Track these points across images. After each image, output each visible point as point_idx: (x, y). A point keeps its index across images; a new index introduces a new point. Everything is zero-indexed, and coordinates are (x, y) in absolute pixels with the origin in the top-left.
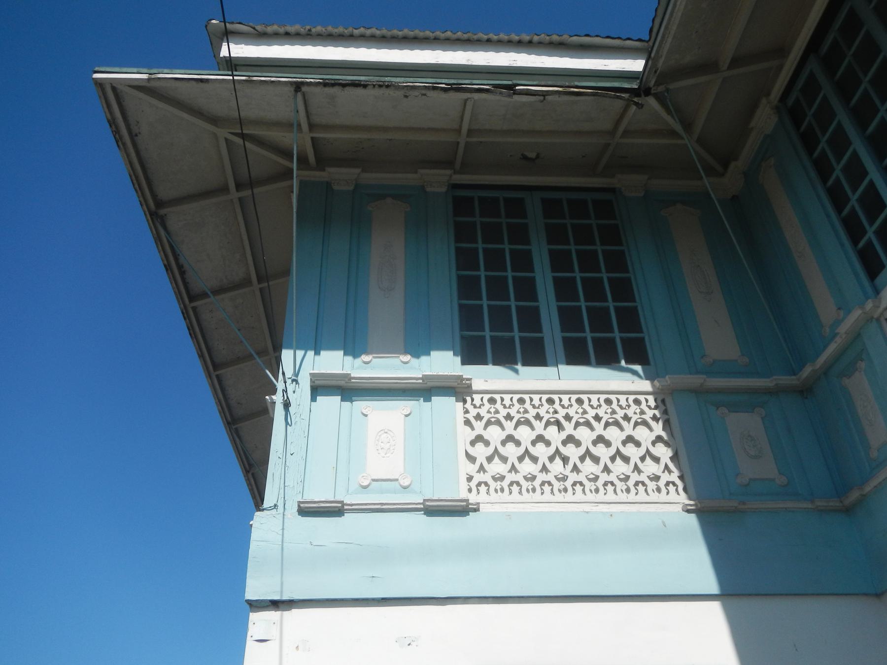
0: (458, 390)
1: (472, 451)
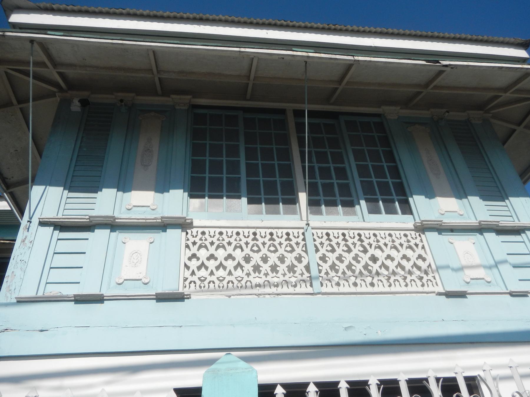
0: (184, 225)
1: (188, 263)
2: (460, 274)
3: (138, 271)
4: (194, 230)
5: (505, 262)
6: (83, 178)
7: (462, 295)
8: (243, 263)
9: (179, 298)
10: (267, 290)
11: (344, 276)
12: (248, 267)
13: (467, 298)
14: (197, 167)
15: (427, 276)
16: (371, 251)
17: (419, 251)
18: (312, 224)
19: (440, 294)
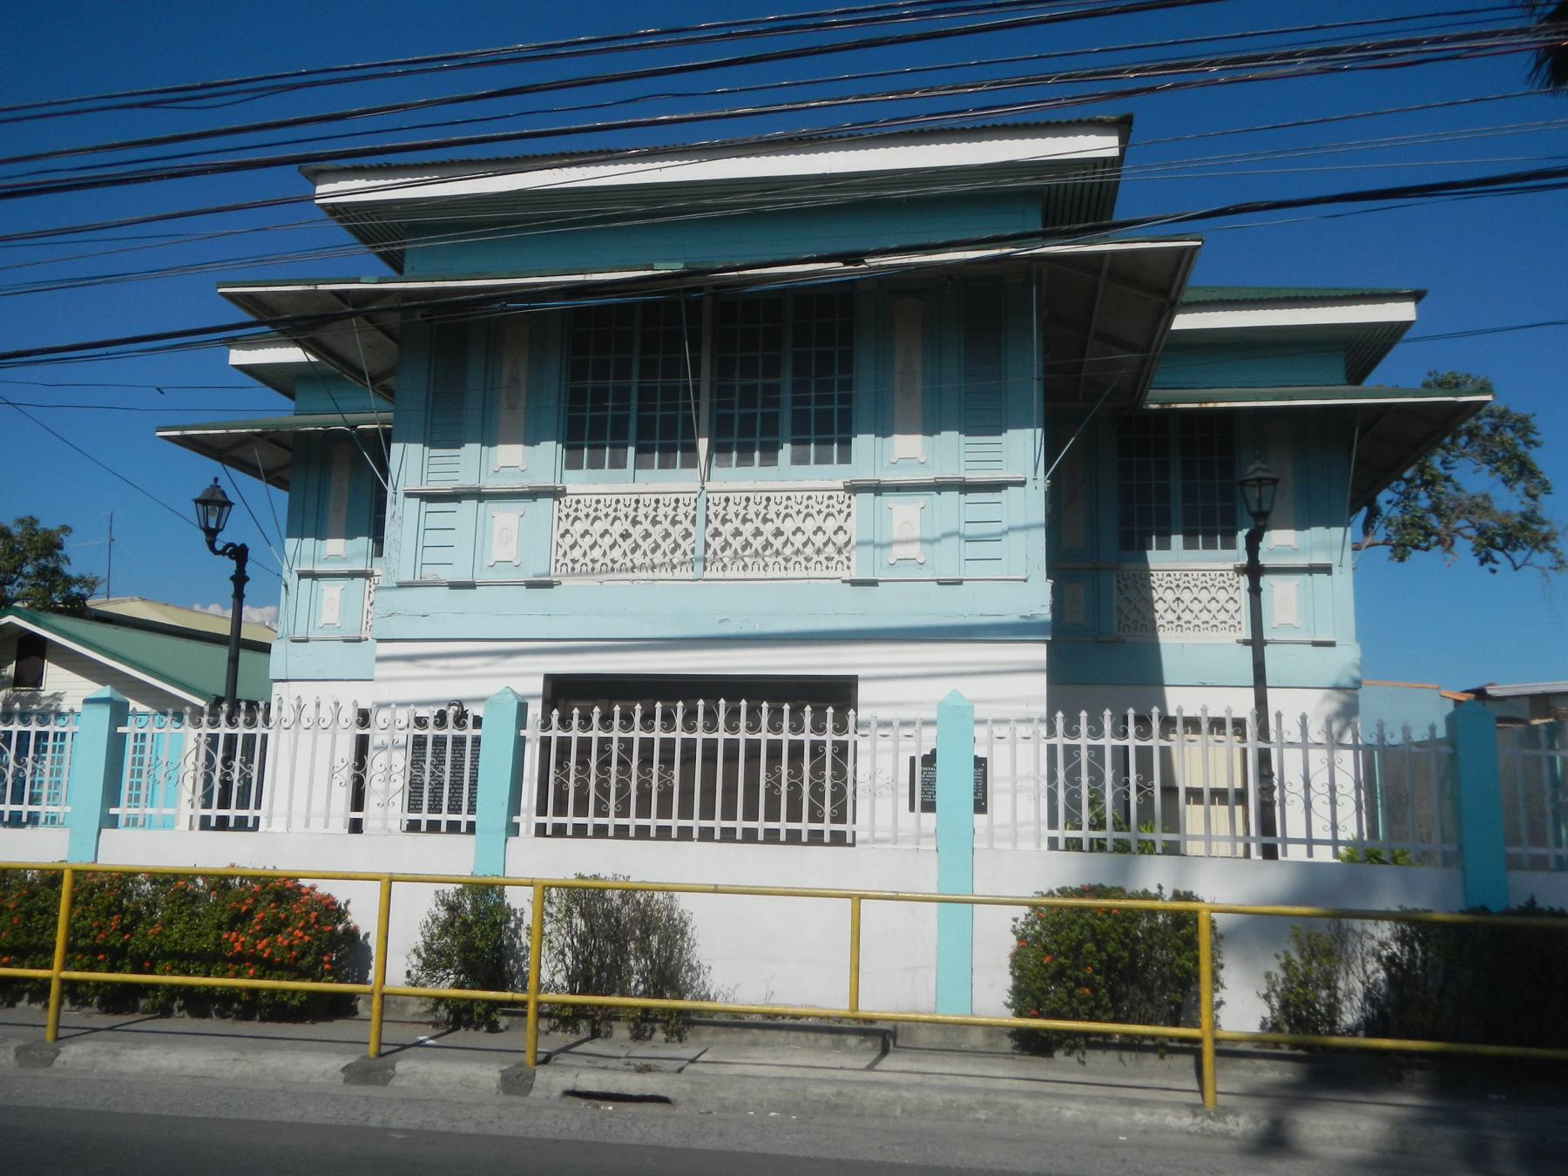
0: (556, 494)
2: (886, 551)
4: (568, 498)
6: (444, 432)
9: (549, 585)
14: (576, 398)
18: (708, 486)
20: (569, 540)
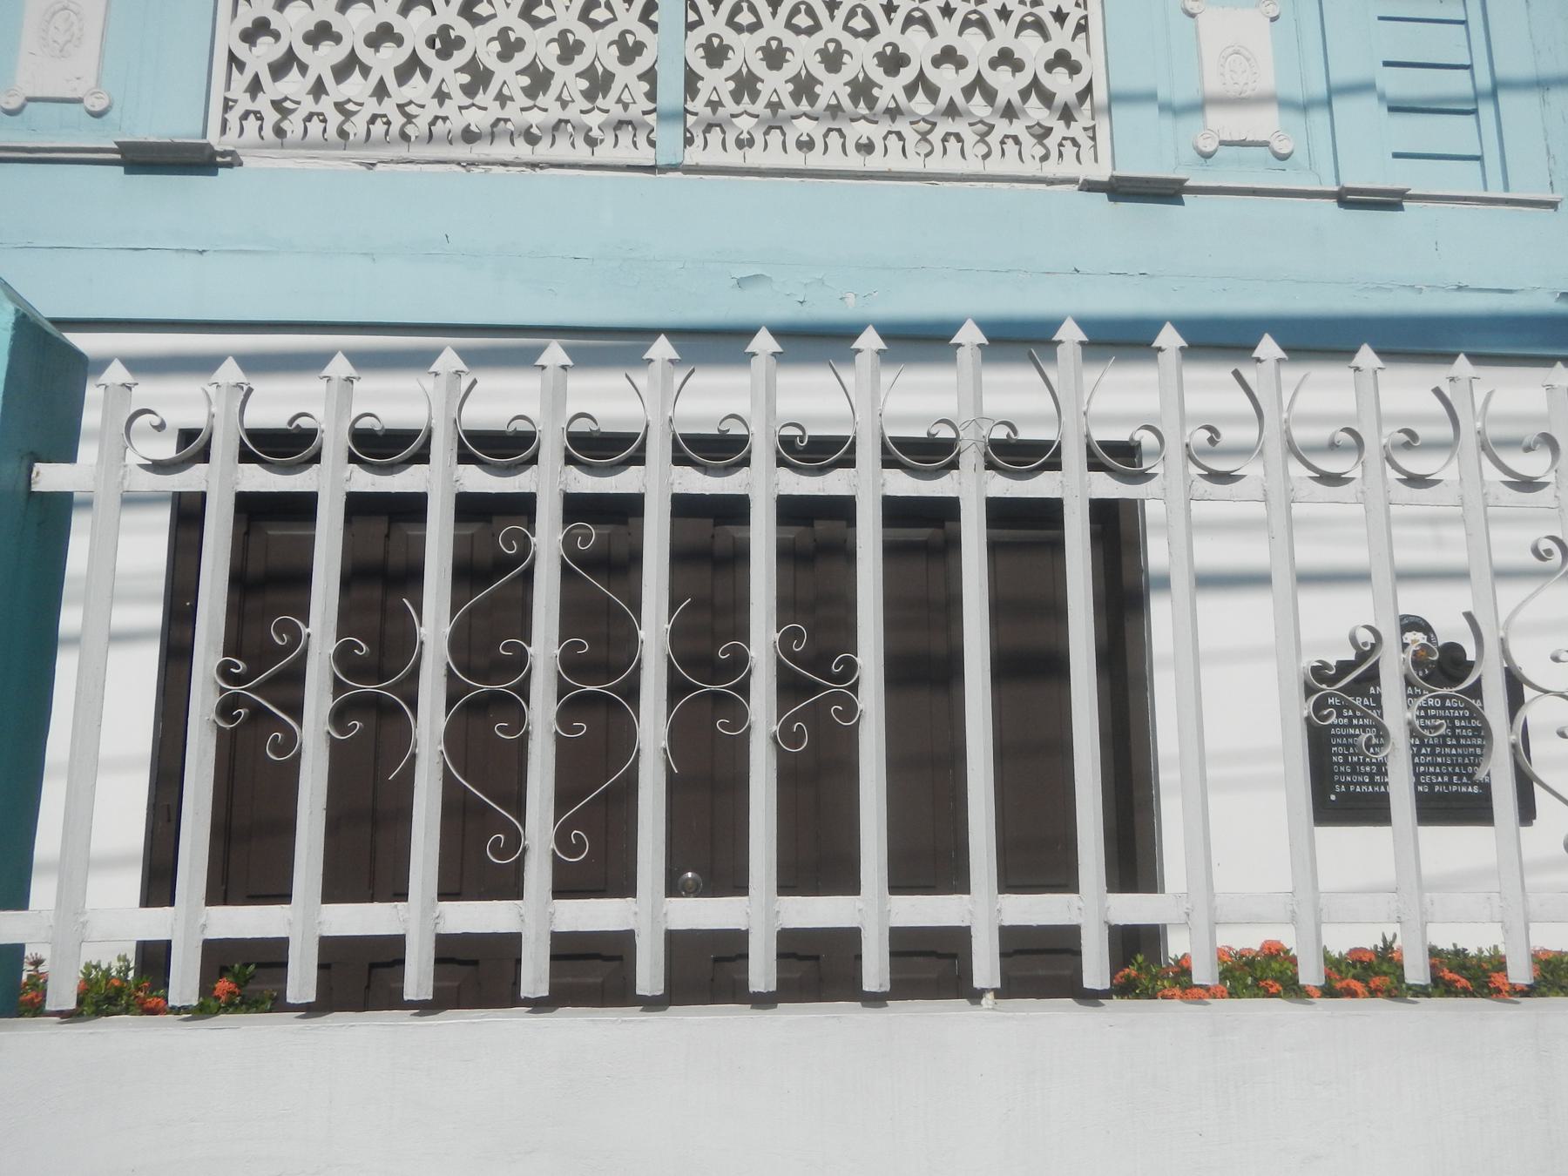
1: (241, 50)
2: (1189, 124)
3: (73, 73)
5: (1366, 87)
7: (1167, 192)
8: (428, 56)
10: (502, 150)
11: (775, 113)
12: (448, 72)
13: (1182, 203)
15: (1068, 126)
16: (889, 32)
17: (1061, 37)
19: (1090, 186)
20: (265, 52)
